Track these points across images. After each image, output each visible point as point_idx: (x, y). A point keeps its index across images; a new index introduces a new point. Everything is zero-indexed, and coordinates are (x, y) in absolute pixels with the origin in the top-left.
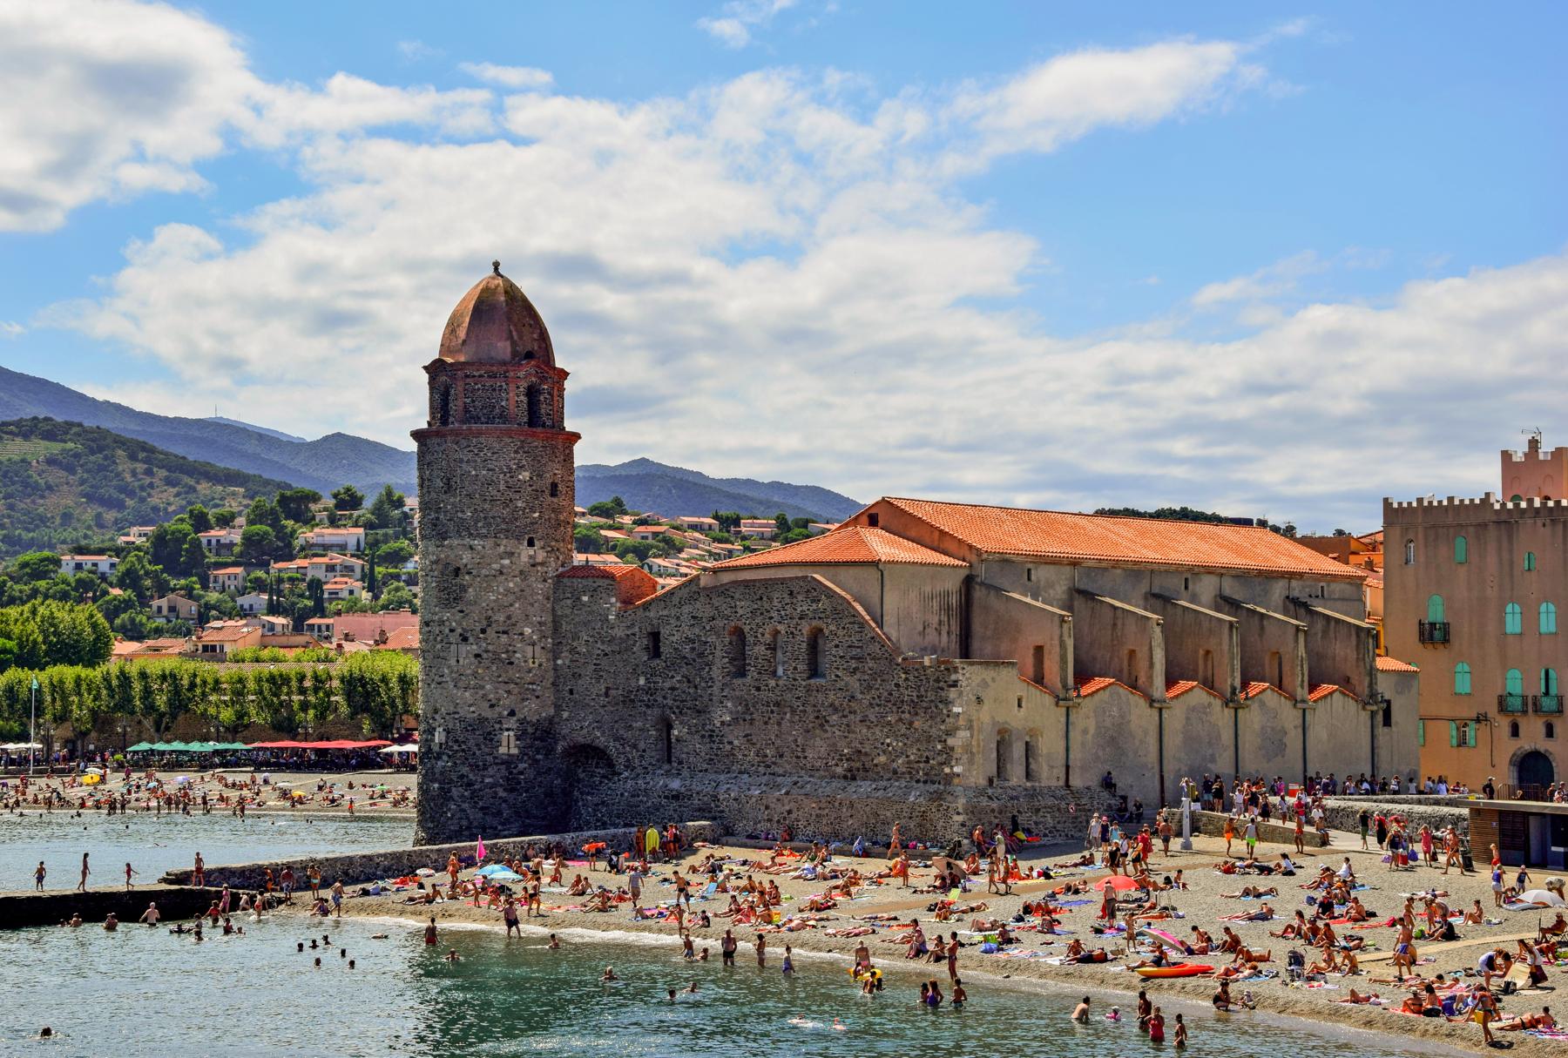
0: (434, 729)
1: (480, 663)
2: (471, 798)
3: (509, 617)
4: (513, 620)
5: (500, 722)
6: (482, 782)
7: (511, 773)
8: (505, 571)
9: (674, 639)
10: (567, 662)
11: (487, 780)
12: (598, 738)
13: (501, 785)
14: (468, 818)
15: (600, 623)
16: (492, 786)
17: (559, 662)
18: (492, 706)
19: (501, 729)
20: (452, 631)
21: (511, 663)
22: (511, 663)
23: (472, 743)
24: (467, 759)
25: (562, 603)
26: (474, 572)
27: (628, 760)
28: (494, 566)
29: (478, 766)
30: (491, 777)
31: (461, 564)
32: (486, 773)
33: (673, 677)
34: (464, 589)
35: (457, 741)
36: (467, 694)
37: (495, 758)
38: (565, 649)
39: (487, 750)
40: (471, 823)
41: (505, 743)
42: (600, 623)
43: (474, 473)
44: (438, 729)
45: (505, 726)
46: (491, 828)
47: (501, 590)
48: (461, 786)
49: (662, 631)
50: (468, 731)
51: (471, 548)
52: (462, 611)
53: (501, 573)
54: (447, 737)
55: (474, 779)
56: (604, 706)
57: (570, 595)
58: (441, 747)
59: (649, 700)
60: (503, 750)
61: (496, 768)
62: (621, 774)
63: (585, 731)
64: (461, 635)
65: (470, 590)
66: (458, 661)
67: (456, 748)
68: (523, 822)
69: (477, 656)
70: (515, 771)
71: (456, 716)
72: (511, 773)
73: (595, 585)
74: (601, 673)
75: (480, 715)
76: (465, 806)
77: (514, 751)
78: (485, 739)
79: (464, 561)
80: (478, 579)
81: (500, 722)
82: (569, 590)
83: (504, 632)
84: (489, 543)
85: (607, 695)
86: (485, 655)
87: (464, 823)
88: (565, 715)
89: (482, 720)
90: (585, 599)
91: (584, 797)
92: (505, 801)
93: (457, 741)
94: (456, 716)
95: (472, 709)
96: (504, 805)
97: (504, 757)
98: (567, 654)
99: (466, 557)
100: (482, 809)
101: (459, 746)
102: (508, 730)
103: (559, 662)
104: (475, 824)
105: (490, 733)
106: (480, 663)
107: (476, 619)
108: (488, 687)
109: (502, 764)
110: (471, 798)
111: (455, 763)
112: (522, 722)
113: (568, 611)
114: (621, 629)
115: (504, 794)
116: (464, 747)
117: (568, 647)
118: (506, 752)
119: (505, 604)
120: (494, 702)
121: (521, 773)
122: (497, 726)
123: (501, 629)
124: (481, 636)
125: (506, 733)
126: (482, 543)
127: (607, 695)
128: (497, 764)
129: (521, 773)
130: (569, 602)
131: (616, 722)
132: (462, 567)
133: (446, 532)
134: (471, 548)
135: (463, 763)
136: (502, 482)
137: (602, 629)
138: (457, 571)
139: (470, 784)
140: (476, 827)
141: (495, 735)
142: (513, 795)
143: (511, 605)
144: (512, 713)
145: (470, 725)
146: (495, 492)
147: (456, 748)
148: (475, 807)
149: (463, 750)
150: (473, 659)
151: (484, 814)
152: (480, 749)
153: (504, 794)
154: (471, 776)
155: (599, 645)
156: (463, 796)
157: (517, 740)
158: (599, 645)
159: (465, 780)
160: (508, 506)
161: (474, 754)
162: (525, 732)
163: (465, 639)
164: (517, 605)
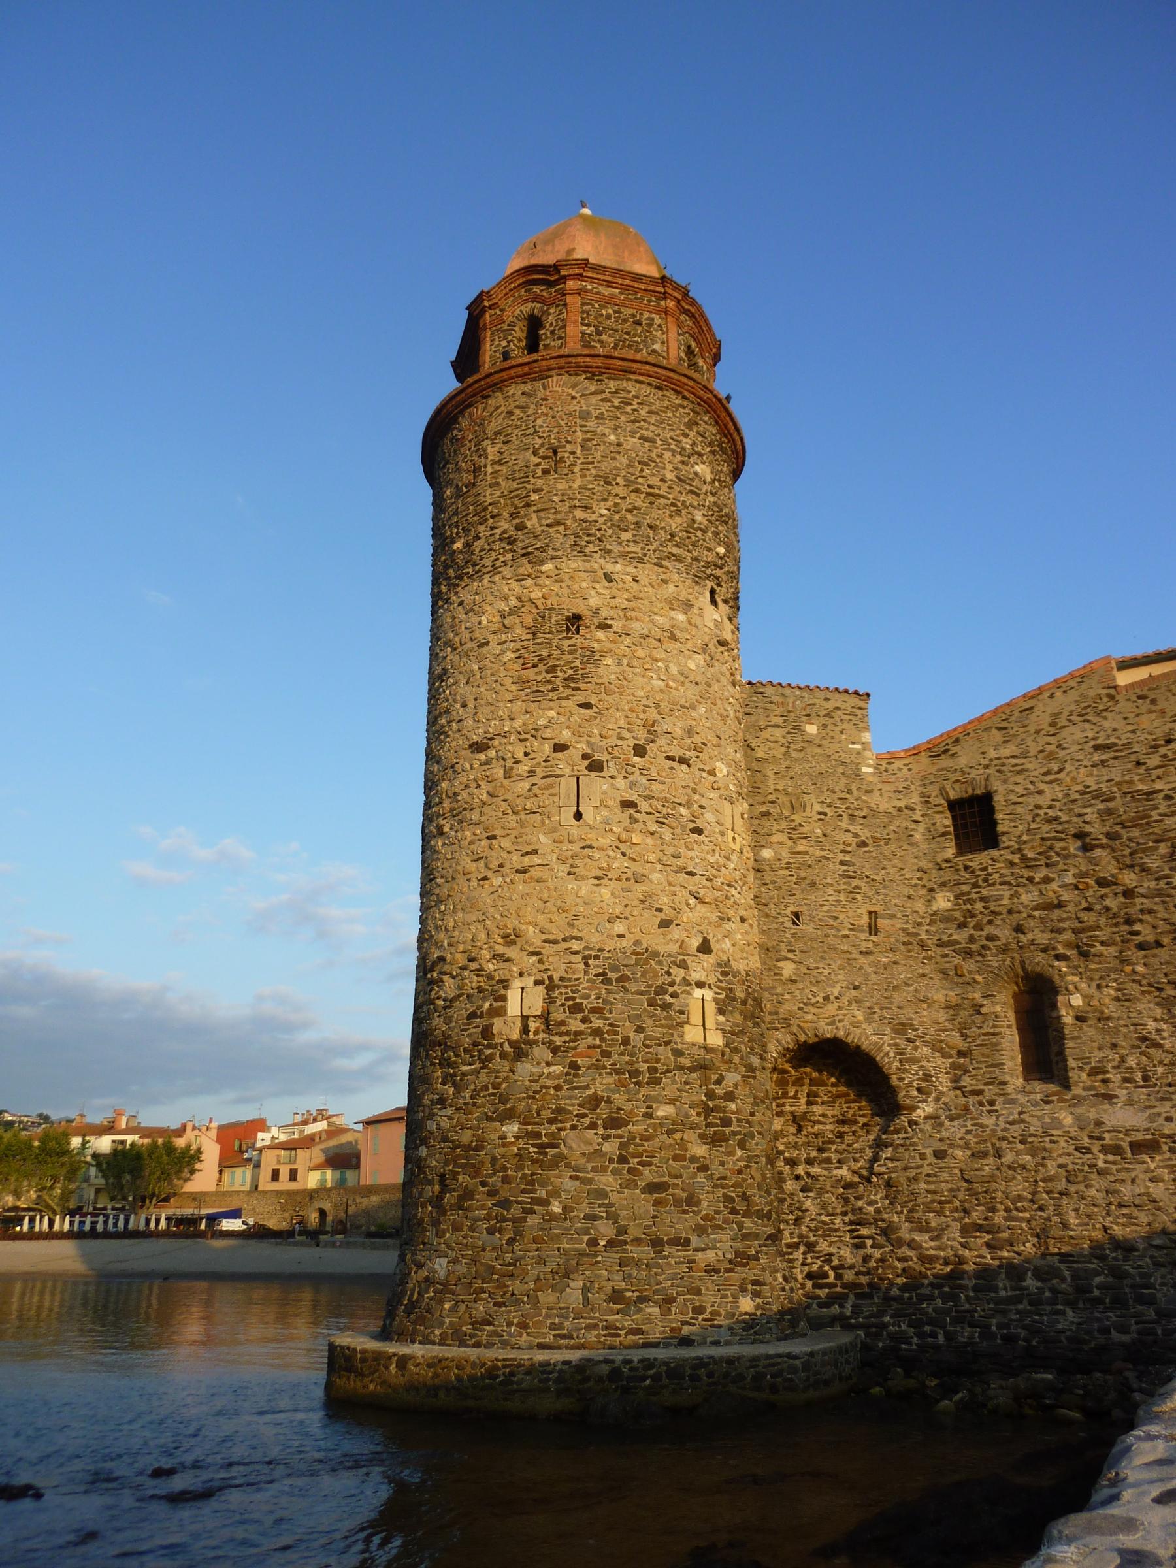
0: (505, 983)
1: (634, 820)
2: (623, 1160)
3: (690, 732)
4: (698, 739)
5: (683, 965)
6: (648, 1115)
7: (710, 1095)
8: (678, 634)
9: (1044, 801)
10: (785, 854)
11: (663, 1111)
12: (857, 1025)
13: (694, 1127)
14: (613, 1217)
15: (843, 781)
16: (674, 1127)
17: (767, 853)
18: (665, 924)
19: (686, 982)
20: (559, 748)
21: (698, 831)
22: (698, 831)
23: (618, 1012)
24: (607, 1054)
25: (766, 734)
26: (617, 625)
27: (927, 1077)
28: (661, 620)
29: (635, 1073)
30: (671, 1102)
31: (579, 607)
32: (654, 1091)
33: (1047, 880)
34: (592, 658)
35: (577, 1008)
36: (605, 892)
37: (678, 1053)
38: (776, 827)
39: (659, 1032)
40: (622, 1231)
41: (696, 1018)
42: (843, 781)
43: (612, 437)
44: (517, 984)
45: (695, 976)
46: (675, 1242)
47: (674, 670)
48: (593, 1126)
49: (997, 786)
50: (606, 981)
51: (608, 578)
52: (587, 706)
53: (673, 638)
54: (550, 1000)
55: (627, 1107)
56: (868, 953)
57: (780, 721)
58: (525, 1030)
59: (972, 939)
60: (692, 1034)
61: (681, 1078)
62: (913, 1108)
63: (832, 1008)
64: (585, 756)
65: (608, 661)
66: (578, 816)
67: (575, 1025)
68: (741, 1226)
69: (627, 804)
70: (719, 1090)
71: (575, 945)
72: (710, 1095)
73: (830, 705)
74: (856, 882)
75: (637, 943)
76: (607, 1181)
77: (716, 1040)
78: (651, 1003)
79: (594, 602)
80: (627, 641)
81: (683, 965)
82: (779, 710)
83: (683, 761)
84: (647, 574)
85: (873, 929)
86: (644, 806)
87: (606, 1230)
88: (788, 969)
89: (643, 956)
90: (811, 729)
91: (800, 1170)
92: (704, 1168)
93: (577, 1008)
94: (575, 945)
95: (619, 928)
96: (701, 1178)
97: (699, 1053)
98: (782, 838)
99: (595, 598)
100: (652, 1188)
101: (584, 1020)
102: (700, 985)
103: (767, 853)
104: (634, 1232)
105: (661, 990)
106: (634, 820)
107: (622, 723)
108: (655, 876)
109: (692, 1069)
110: (623, 1160)
111: (575, 1067)
112: (725, 969)
113: (779, 752)
114: (886, 795)
115: (699, 1150)
116: (597, 1023)
117: (784, 824)
118: (699, 1039)
119: (683, 702)
120: (668, 913)
121: (730, 1096)
122: (678, 974)
123: (676, 752)
124: (637, 759)
125: (698, 993)
126: (631, 569)
127: (873, 929)
128: (681, 1068)
129: (730, 1096)
130: (779, 733)
131: (896, 988)
132: (586, 613)
133: (542, 550)
134: (608, 578)
135: (598, 1067)
136: (669, 467)
137: (850, 792)
138: (576, 618)
139: (615, 1122)
140: (637, 1241)
141: (674, 995)
142: (719, 1154)
143: (693, 707)
144: (705, 948)
145: (614, 968)
146: (654, 481)
147: (575, 1025)
148: (629, 1185)
149: (597, 1032)
150: (618, 810)
151: (657, 1203)
152: (640, 1029)
153: (699, 1150)
154: (619, 1099)
155: (844, 824)
156: (599, 1153)
157: (721, 1011)
158: (844, 824)
159: (603, 1111)
160: (678, 513)
161: (626, 1041)
162: (731, 997)
163: (596, 767)
164: (702, 709)
